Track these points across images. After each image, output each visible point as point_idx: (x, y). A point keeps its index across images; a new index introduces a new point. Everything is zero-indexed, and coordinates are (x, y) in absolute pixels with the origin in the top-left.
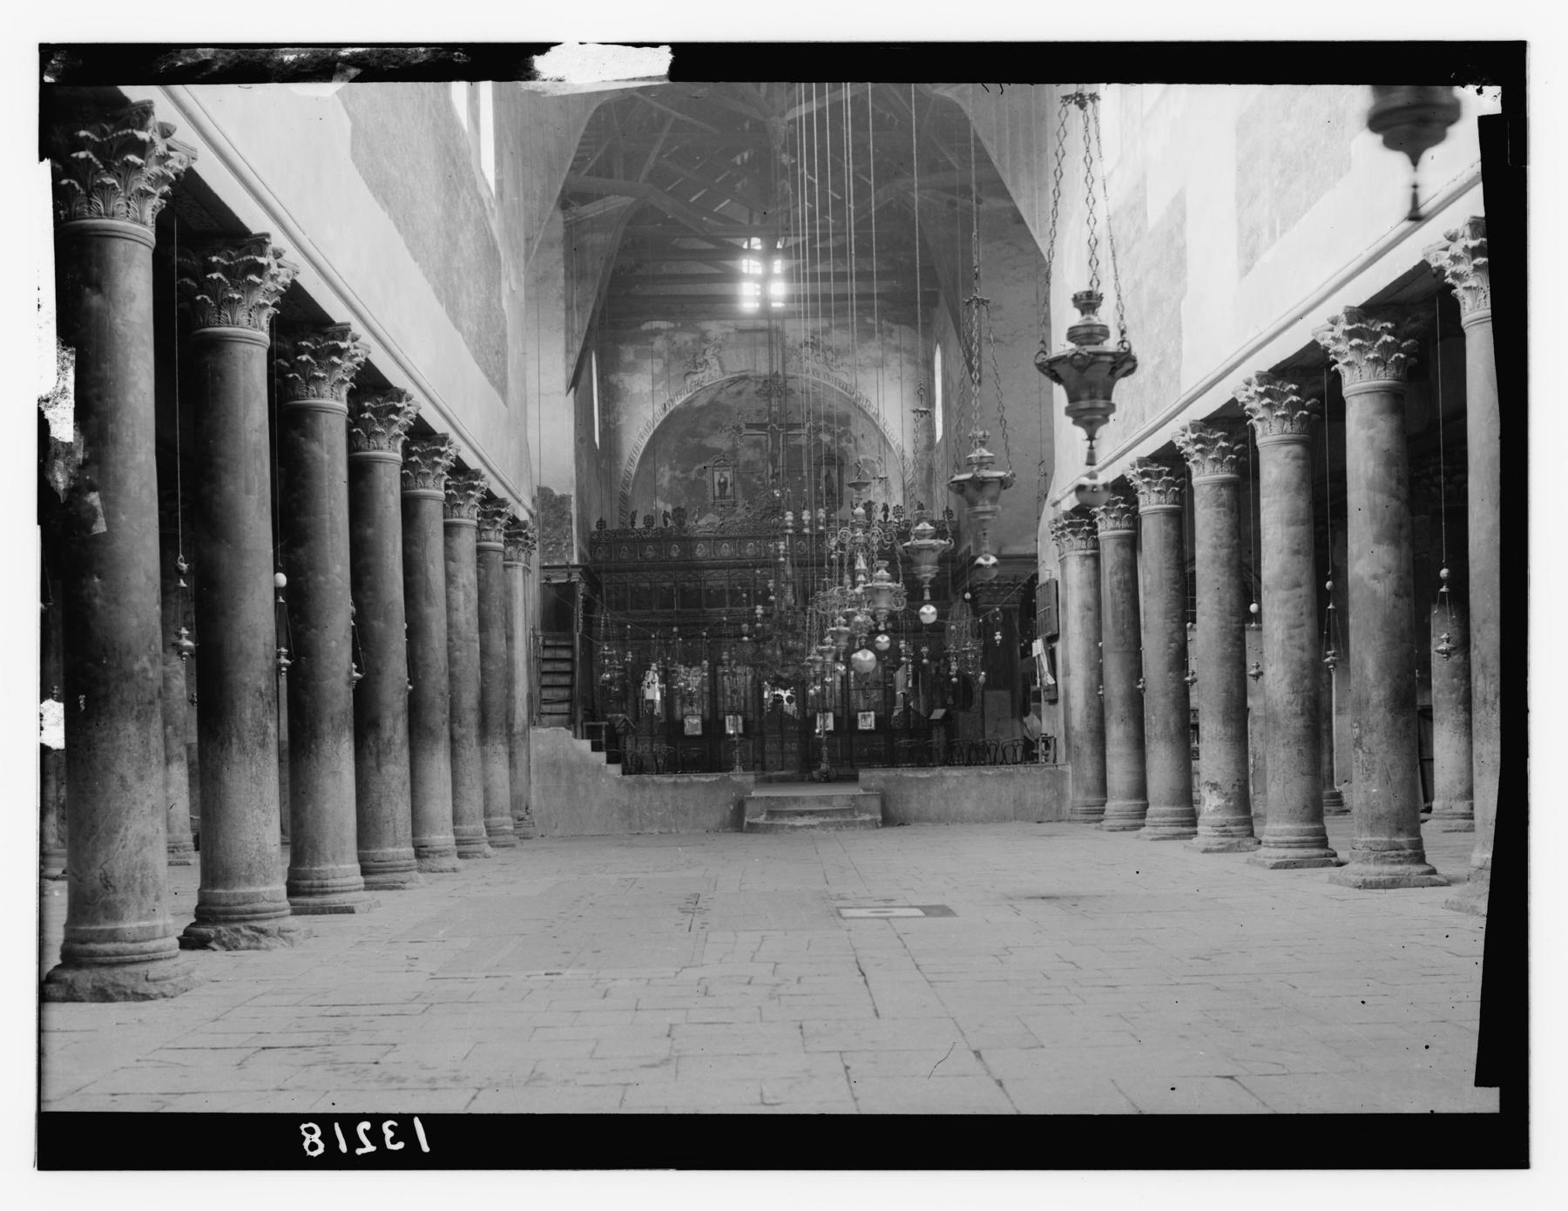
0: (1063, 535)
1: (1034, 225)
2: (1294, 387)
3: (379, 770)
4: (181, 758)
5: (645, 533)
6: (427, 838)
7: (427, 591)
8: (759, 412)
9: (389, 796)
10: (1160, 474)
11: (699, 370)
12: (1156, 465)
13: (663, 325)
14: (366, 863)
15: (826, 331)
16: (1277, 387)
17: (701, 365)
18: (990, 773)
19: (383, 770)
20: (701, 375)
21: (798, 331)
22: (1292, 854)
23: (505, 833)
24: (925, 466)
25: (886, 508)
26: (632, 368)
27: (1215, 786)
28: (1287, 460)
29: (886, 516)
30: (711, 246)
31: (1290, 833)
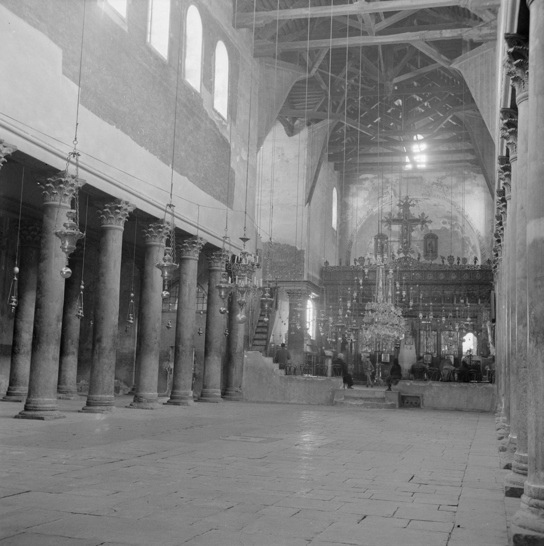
1: (489, 125)
3: (99, 360)
4: (74, 353)
5: (346, 268)
6: (143, 394)
7: (152, 285)
9: (102, 372)
11: (385, 196)
13: (370, 176)
14: (89, 401)
17: (385, 193)
18: (455, 386)
19: (101, 361)
20: (385, 198)
21: (430, 178)
23: (216, 396)
24: (490, 240)
25: (459, 259)
26: (355, 195)
29: (458, 263)
30: (385, 141)
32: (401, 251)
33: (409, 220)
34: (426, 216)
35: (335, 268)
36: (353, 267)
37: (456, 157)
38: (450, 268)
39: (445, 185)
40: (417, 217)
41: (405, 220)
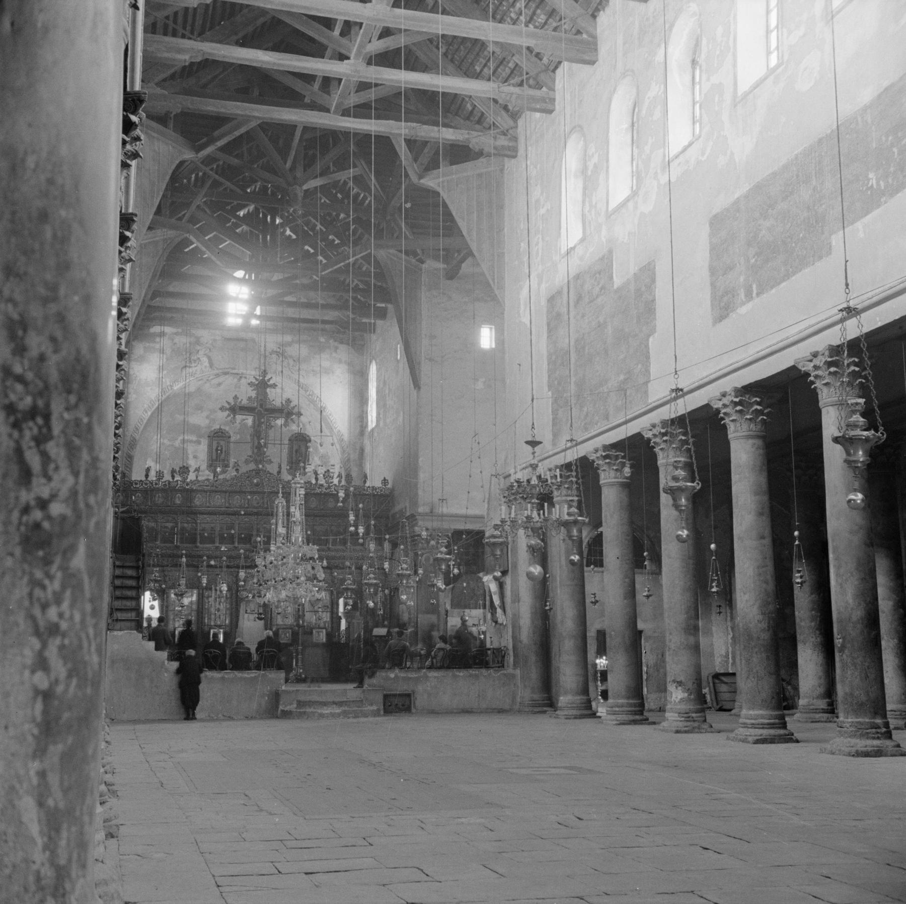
0: (515, 499)
2: (758, 399)
8: (250, 398)
10: (617, 457)
11: (193, 365)
12: (614, 451)
13: (168, 330)
15: (289, 344)
16: (746, 398)
17: (195, 361)
18: (461, 674)
20: (194, 369)
21: (272, 342)
22: (766, 732)
24: (358, 447)
26: (142, 359)
27: (680, 683)
28: (753, 450)
31: (762, 717)
32: (251, 459)
33: (267, 410)
34: (292, 405)
35: (136, 484)
36: (169, 482)
37: (291, 312)
38: (326, 489)
39: (291, 357)
40: (278, 403)
41: (259, 408)
